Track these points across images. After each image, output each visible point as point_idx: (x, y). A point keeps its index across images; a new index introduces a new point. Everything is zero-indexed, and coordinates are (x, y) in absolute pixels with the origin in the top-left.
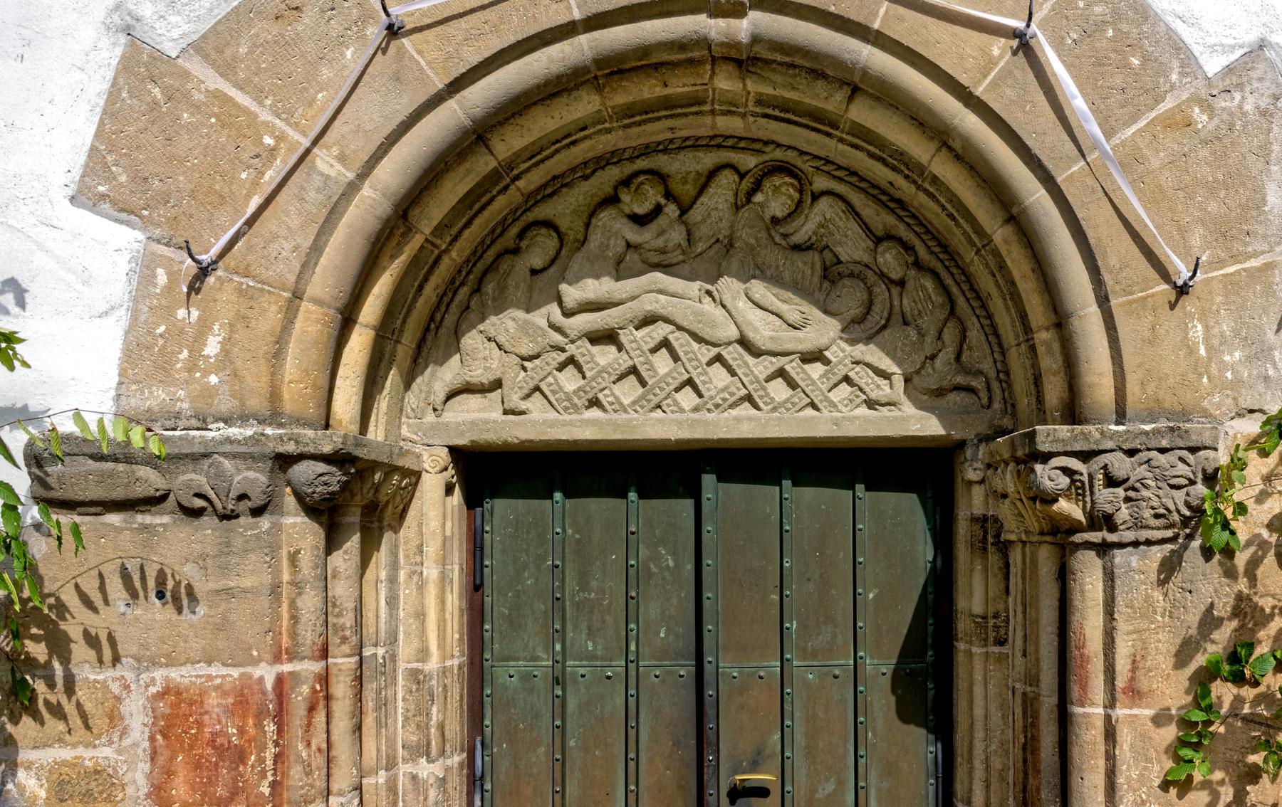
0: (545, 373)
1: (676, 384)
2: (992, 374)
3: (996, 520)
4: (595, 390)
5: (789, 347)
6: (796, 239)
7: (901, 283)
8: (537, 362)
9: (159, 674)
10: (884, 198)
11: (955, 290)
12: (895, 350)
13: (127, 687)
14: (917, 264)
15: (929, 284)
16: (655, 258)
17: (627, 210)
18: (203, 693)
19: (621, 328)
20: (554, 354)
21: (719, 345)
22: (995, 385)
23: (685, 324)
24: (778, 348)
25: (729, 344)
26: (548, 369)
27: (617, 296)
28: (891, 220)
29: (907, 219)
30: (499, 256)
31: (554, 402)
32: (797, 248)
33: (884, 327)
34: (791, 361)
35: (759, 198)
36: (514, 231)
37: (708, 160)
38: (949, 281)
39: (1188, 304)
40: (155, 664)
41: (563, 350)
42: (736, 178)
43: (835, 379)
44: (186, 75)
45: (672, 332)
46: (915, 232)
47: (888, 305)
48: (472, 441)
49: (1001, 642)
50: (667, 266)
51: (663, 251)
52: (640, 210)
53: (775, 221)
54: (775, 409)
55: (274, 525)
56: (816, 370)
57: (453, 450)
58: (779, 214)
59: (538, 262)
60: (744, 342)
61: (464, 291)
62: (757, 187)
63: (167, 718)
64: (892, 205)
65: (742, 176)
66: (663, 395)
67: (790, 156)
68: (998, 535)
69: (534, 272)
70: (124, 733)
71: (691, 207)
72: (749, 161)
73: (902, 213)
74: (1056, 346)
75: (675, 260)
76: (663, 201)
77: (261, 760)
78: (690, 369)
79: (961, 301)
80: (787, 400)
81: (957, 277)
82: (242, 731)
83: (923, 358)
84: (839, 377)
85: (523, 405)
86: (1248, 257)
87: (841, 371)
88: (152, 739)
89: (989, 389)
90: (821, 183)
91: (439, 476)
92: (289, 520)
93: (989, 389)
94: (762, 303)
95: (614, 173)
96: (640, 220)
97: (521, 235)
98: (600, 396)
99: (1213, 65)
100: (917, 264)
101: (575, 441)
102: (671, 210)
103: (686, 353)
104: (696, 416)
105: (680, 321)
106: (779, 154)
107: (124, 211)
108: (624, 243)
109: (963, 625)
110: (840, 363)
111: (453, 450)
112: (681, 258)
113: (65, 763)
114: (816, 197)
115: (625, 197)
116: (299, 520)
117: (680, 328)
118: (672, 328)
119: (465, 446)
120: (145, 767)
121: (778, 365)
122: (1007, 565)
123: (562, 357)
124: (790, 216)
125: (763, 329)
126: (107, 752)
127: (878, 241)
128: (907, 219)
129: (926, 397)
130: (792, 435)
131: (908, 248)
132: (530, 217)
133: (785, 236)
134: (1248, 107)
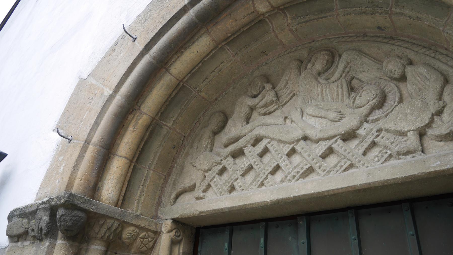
0: (212, 177)
1: (270, 169)
4: (232, 181)
5: (332, 133)
7: (403, 78)
8: (210, 172)
10: (380, 39)
11: (444, 67)
12: (406, 115)
16: (263, 111)
17: (250, 94)
19: (245, 147)
20: (217, 167)
21: (293, 143)
23: (274, 136)
24: (326, 135)
25: (298, 140)
26: (214, 174)
27: (243, 132)
29: (397, 44)
31: (216, 191)
34: (336, 141)
38: (438, 64)
41: (220, 163)
43: (366, 145)
45: (269, 143)
46: (406, 48)
47: (398, 94)
48: (181, 215)
50: (270, 113)
51: (266, 106)
54: (329, 172)
56: (353, 144)
57: (175, 221)
60: (305, 138)
64: (386, 40)
66: (264, 176)
73: (394, 42)
75: (272, 110)
78: (278, 159)
80: (336, 166)
81: (443, 60)
83: (430, 115)
84: (368, 143)
85: (202, 195)
87: (369, 140)
91: (168, 234)
94: (314, 114)
98: (235, 184)
101: (222, 209)
103: (276, 151)
104: (280, 185)
105: (271, 136)
108: (248, 108)
110: (368, 134)
111: (175, 221)
112: (275, 107)
117: (272, 139)
118: (269, 140)
119: (178, 218)
121: (328, 145)
123: (220, 167)
125: (316, 126)
128: (397, 44)
129: (442, 144)
130: (340, 187)
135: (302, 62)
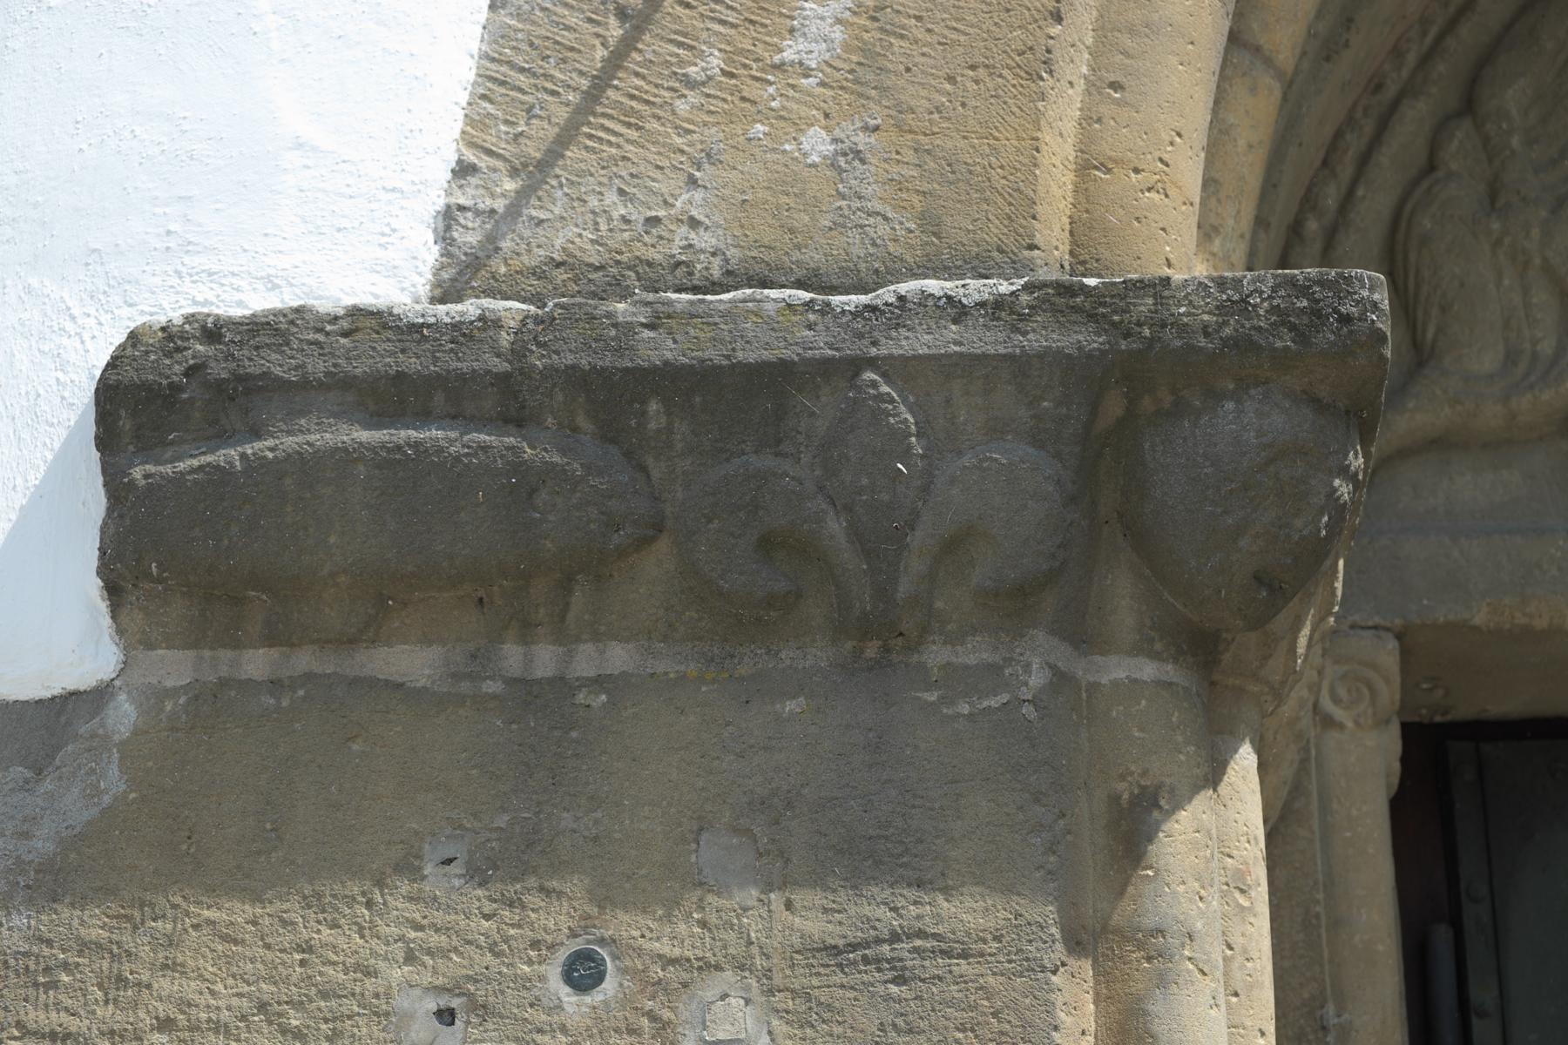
55: (1061, 679)
92: (1116, 669)
116: (1148, 670)
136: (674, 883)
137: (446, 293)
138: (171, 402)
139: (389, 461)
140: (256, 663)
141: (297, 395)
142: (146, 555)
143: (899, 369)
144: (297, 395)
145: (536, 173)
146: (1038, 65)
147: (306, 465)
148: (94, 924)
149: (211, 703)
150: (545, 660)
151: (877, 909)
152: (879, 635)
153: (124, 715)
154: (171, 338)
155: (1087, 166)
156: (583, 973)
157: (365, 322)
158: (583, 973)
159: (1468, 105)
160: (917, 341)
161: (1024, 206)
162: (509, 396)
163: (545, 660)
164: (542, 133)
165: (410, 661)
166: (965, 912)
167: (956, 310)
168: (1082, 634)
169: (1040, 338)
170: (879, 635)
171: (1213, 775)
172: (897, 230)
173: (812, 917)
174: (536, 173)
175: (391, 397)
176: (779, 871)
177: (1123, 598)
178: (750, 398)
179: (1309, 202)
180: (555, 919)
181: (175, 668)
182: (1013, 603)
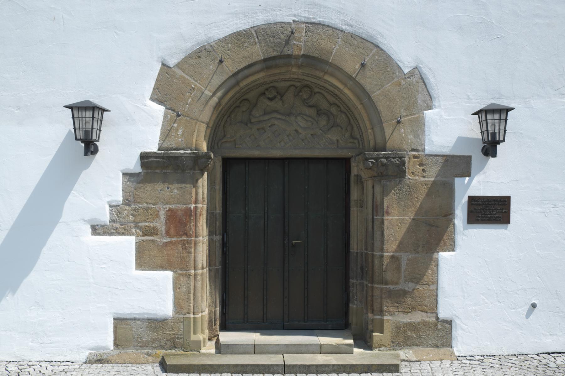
2: (360, 139)
3: (360, 176)
6: (310, 104)
9: (167, 206)
11: (350, 117)
13: (160, 209)
14: (341, 111)
15: (344, 116)
18: (177, 210)
22: (360, 142)
28: (334, 99)
30: (235, 108)
32: (310, 106)
33: (332, 127)
35: (301, 94)
36: (239, 102)
37: (288, 84)
38: (349, 115)
39: (401, 125)
40: (166, 203)
42: (295, 88)
44: (174, 72)
49: (362, 207)
52: (270, 96)
53: (305, 99)
55: (193, 173)
58: (306, 98)
59: (244, 109)
61: (226, 117)
62: (300, 91)
63: (169, 216)
65: (296, 88)
67: (309, 83)
68: (361, 180)
69: (243, 112)
70: (160, 219)
71: (283, 95)
72: (298, 84)
74: (372, 133)
76: (276, 94)
77: (190, 226)
79: (352, 120)
82: (186, 219)
86: (414, 114)
88: (166, 221)
89: (359, 143)
90: (316, 90)
92: (196, 172)
93: (359, 143)
95: (265, 87)
96: (271, 99)
97: (240, 103)
99: (406, 71)
100: (341, 111)
102: (279, 97)
106: (306, 82)
107: (160, 102)
109: (352, 203)
113: (146, 226)
114: (315, 93)
115: (267, 93)
120: (164, 227)
122: (363, 187)
124: (308, 98)
126: (155, 224)
127: (331, 104)
131: (339, 107)
132: (243, 98)
133: (307, 103)
134: (414, 81)
135: (296, 88)
136: (173, 183)
137: (159, 150)
138: (144, 157)
139: (156, 161)
140: (149, 171)
141: (151, 157)
142: (143, 165)
143: (184, 157)
144: (151, 157)
145: (164, 141)
146: (193, 135)
147: (152, 161)
148: (142, 185)
149: (147, 173)
150: (165, 171)
151: (184, 185)
152: (183, 171)
153: (142, 174)
154: (144, 153)
155: (196, 140)
156: (168, 188)
157: (154, 152)
158: (168, 188)
159: (229, 116)
160: (185, 155)
161: (192, 144)
162: (163, 157)
163: (165, 171)
164: (164, 138)
165: (158, 171)
166: (188, 185)
167: (187, 153)
168: (195, 170)
169: (192, 155)
170: (183, 171)
171: (203, 174)
172: (184, 146)
173: (180, 186)
174: (164, 141)
175: (156, 157)
176: (178, 183)
177: (197, 168)
178: (177, 158)
179: (218, 124)
180: (166, 186)
181: (145, 171)
182: (191, 169)
